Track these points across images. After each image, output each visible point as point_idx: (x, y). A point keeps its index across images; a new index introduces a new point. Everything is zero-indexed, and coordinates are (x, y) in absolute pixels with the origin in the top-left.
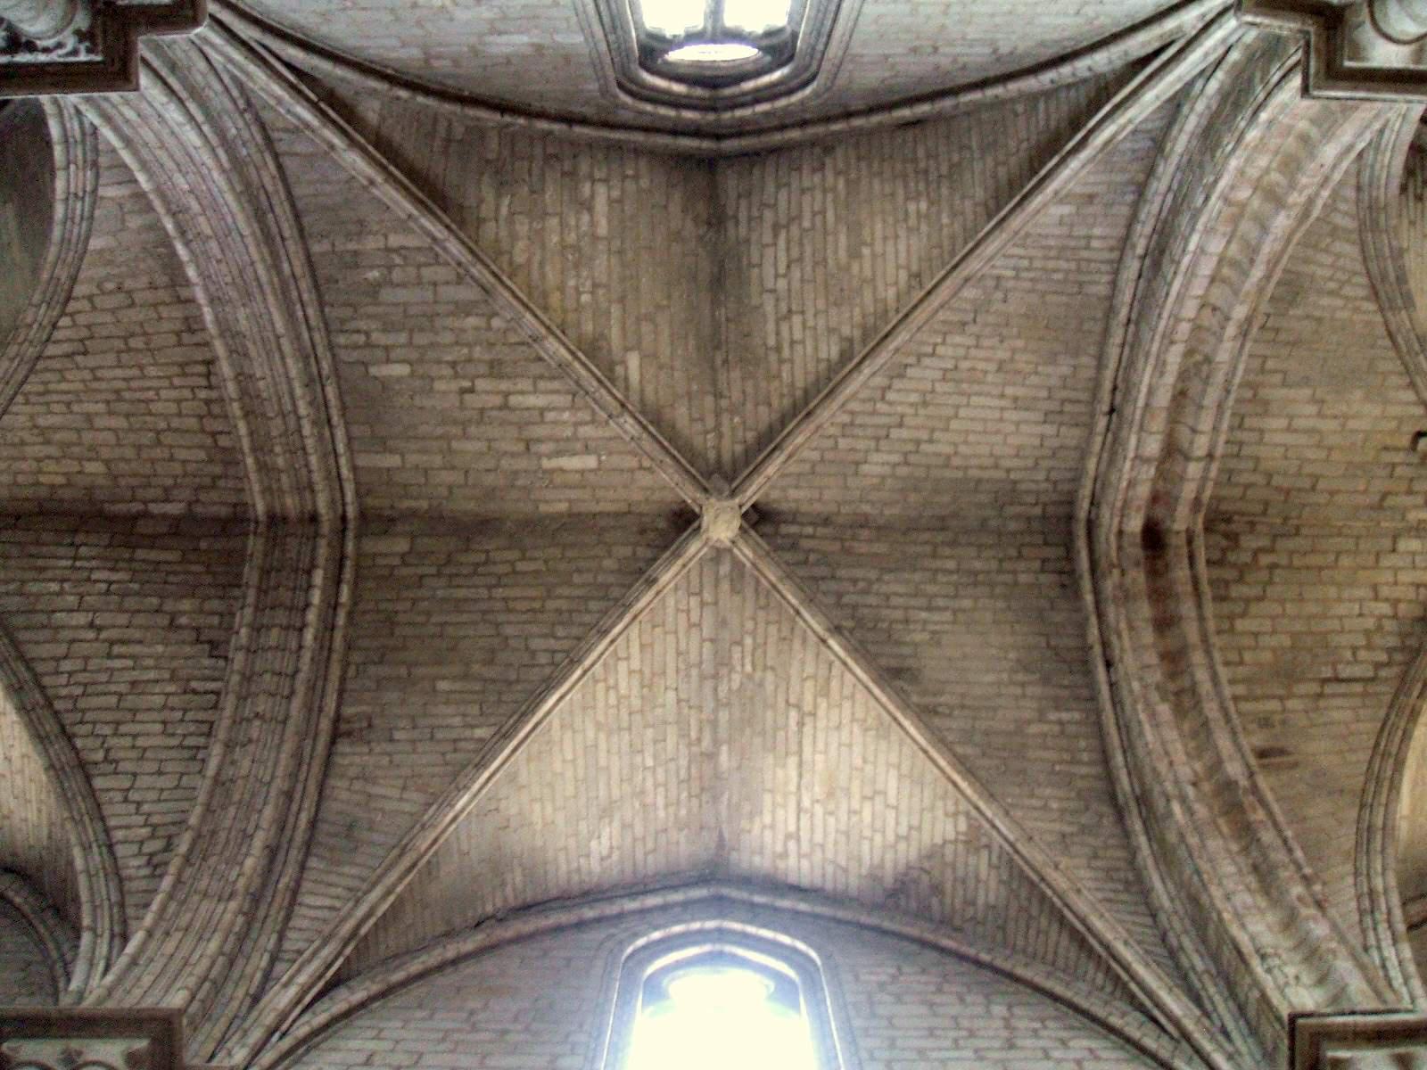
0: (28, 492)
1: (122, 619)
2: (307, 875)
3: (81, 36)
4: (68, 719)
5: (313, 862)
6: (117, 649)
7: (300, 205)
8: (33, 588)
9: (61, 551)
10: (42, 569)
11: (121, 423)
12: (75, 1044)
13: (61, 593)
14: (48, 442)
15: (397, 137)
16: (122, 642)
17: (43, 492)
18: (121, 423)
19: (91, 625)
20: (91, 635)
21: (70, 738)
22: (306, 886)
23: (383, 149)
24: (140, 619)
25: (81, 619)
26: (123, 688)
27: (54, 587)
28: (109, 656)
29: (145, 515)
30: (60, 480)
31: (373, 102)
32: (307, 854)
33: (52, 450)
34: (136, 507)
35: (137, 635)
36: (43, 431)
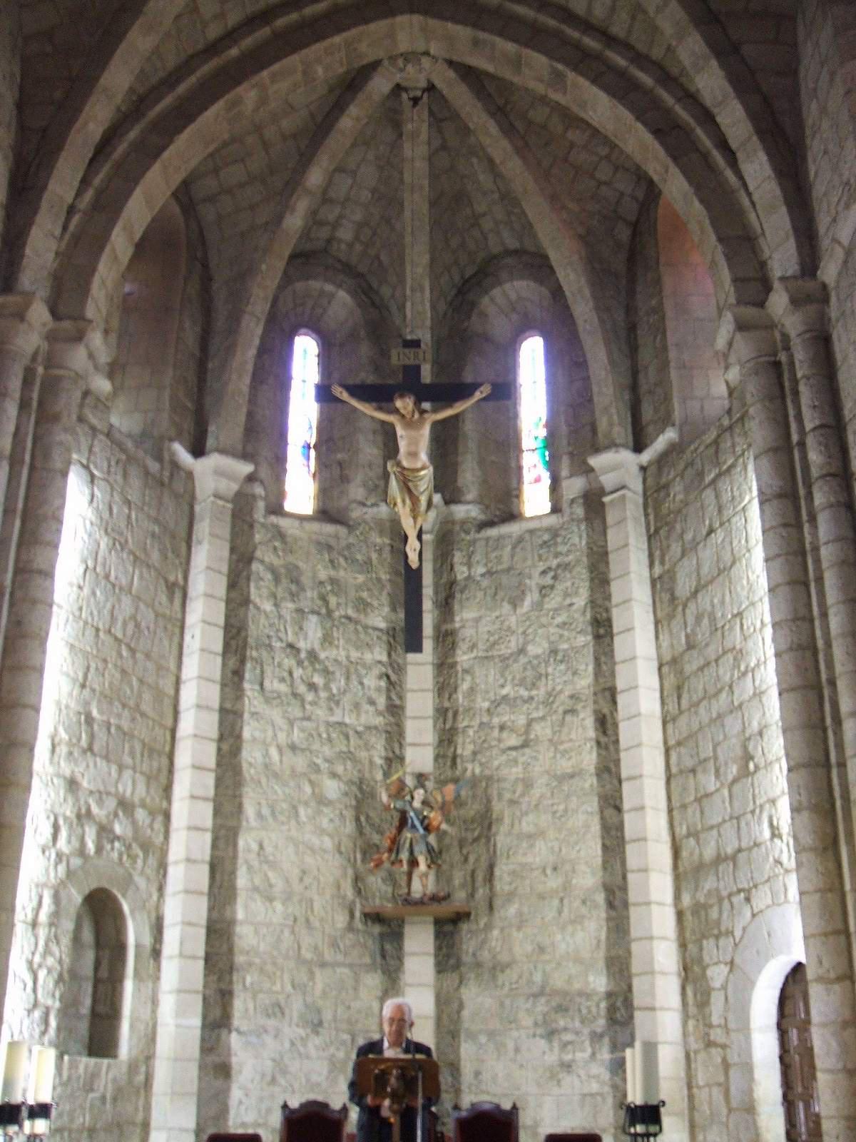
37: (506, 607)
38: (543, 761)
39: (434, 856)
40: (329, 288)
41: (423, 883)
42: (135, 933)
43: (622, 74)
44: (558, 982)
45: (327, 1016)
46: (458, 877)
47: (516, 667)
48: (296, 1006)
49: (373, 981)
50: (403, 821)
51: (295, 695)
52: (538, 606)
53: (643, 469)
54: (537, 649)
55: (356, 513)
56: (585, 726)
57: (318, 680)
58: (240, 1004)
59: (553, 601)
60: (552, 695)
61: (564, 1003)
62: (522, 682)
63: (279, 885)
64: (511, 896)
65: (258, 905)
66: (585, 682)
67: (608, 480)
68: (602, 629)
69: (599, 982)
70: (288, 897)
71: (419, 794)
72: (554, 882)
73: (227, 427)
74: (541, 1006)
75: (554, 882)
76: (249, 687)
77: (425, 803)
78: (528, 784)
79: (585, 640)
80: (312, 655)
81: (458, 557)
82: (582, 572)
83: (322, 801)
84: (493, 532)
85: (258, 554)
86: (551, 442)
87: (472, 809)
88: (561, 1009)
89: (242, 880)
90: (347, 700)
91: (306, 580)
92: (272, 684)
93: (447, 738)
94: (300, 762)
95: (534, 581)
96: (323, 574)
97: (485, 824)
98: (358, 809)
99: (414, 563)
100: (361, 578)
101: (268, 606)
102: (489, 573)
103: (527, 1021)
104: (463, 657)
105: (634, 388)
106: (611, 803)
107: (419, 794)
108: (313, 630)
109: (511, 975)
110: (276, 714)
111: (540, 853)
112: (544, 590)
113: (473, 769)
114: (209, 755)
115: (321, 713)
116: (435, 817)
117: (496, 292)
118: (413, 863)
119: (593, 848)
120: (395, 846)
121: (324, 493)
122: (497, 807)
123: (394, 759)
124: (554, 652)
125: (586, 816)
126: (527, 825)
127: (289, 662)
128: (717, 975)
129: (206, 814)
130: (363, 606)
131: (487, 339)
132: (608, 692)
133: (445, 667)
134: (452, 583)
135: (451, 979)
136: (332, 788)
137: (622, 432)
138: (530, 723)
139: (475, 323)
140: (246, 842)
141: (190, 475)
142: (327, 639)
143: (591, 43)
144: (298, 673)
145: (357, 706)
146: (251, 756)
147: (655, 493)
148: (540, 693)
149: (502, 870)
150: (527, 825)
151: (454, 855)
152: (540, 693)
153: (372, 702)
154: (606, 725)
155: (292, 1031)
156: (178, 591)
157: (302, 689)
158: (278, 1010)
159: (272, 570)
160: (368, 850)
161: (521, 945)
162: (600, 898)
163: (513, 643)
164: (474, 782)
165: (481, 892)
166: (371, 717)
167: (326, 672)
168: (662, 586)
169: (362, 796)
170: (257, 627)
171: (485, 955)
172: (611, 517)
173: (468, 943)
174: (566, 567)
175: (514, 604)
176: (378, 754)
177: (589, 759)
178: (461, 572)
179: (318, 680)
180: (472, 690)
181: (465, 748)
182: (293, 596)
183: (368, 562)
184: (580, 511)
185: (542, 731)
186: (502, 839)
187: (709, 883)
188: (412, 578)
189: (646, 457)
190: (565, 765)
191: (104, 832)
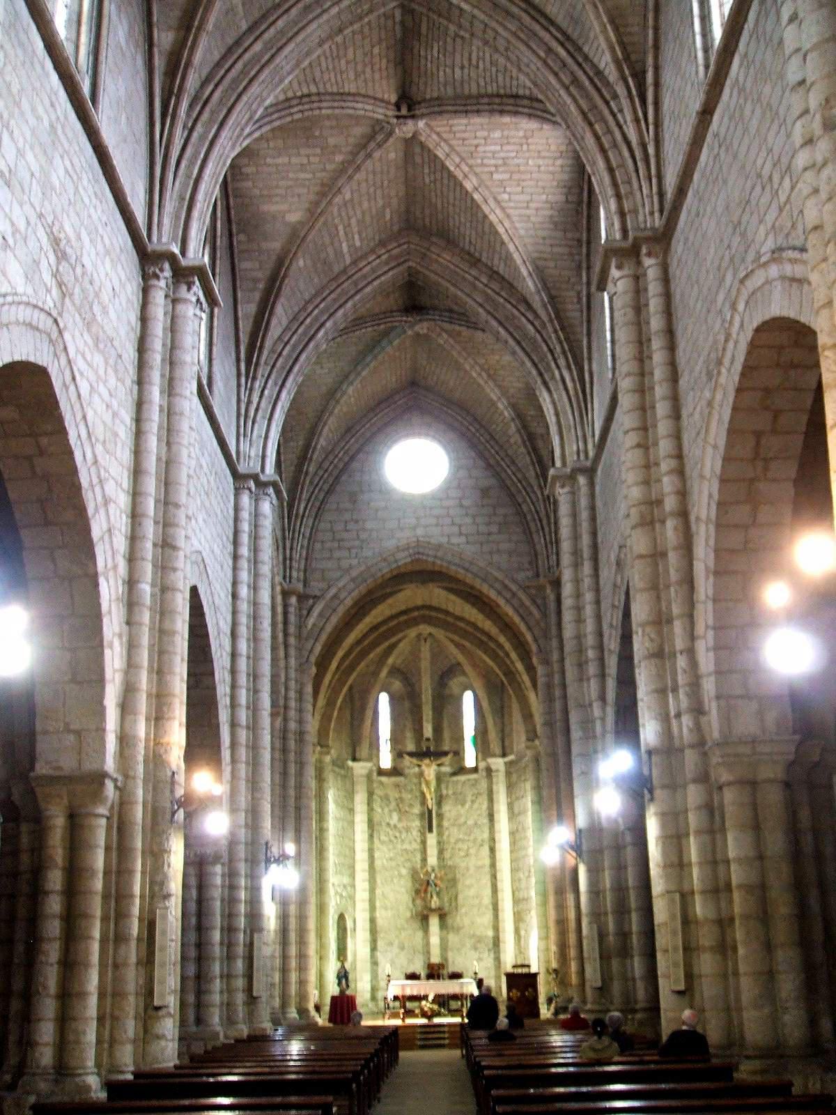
0: (391, 71)
1: (458, 57)
2: (591, 55)
3: (189, 289)
4: (508, 91)
5: (586, 49)
6: (474, 62)
7: (223, 51)
8: (442, 79)
9: (423, 61)
10: (432, 74)
11: (351, 52)
12: (610, 279)
13: (445, 71)
14: (364, 72)
15: (177, 13)
16: (470, 59)
17: (391, 65)
18: (351, 52)
19: (462, 68)
20: (466, 71)
21: (516, 96)
22: (595, 60)
23: (188, 26)
24: (458, 48)
25: (458, 72)
26: (494, 69)
27: (441, 73)
28: (477, 67)
29: (402, 23)
30: (384, 61)
31: (165, 39)
32: (580, 49)
33: (368, 70)
34: (398, 28)
35: (466, 55)
36: (357, 76)
37: (460, 807)
38: (472, 862)
39: (438, 894)
40: (393, 680)
41: (435, 903)
42: (349, 924)
43: (494, 651)
44: (478, 933)
45: (406, 945)
46: (446, 899)
47: (464, 829)
48: (396, 942)
49: (420, 934)
50: (428, 883)
51: (390, 841)
52: (471, 807)
53: (505, 763)
54: (470, 822)
55: (407, 771)
56: (485, 850)
57: (398, 834)
58: (380, 944)
59: (476, 806)
60: (475, 840)
61: (479, 940)
62: (466, 834)
63: (389, 904)
64: (463, 906)
65: (383, 912)
66: (486, 835)
67: (493, 767)
68: (491, 816)
69: (490, 933)
70: (392, 909)
71: (433, 875)
72: (477, 901)
73: (364, 751)
74: (473, 940)
75: (477, 901)
76: (376, 840)
77: (436, 877)
78: (468, 869)
79: (486, 821)
80: (395, 826)
81: (443, 786)
82: (485, 797)
83: (400, 876)
84: (455, 778)
85: (376, 791)
86: (475, 737)
87: (450, 876)
88: (479, 941)
89: (378, 904)
90: (407, 841)
91: (391, 799)
92: (383, 838)
93: (441, 852)
94: (393, 864)
95: (469, 798)
96: (397, 796)
97: (453, 882)
98: (413, 876)
99: (430, 807)
100: (410, 796)
101: (380, 810)
102: (454, 793)
103: (468, 945)
104: (445, 824)
105: (503, 731)
106: (494, 877)
107: (433, 875)
108: (395, 816)
109: (462, 932)
110: (385, 849)
111: (472, 892)
112: (473, 802)
113: (450, 863)
114: (366, 866)
115: (399, 846)
116: (438, 882)
117: (455, 680)
118: (432, 896)
119: (488, 892)
120: (426, 891)
121: (394, 760)
122: (458, 876)
123: (424, 860)
124: (476, 824)
125: (486, 880)
126: (468, 882)
127: (388, 830)
128: (523, 933)
129: (366, 885)
130: (411, 806)
131: (451, 696)
132: (493, 840)
133: (440, 834)
134: (441, 796)
135: (445, 932)
136: (404, 871)
137: (498, 750)
138: (468, 848)
139: (447, 691)
140: (378, 892)
141: (352, 768)
142: (400, 820)
143: (484, 638)
144: (391, 833)
145: (410, 843)
146: (378, 863)
147: (508, 774)
148: (472, 838)
149: (460, 897)
150: (468, 882)
151: (444, 893)
152: (472, 838)
153: (415, 841)
154: (492, 850)
155: (395, 950)
156: (351, 811)
157: (393, 838)
158: (391, 944)
159: (381, 798)
160: (417, 892)
161: (466, 921)
162: (491, 907)
163: (462, 820)
164: (450, 867)
165: (453, 904)
166: (416, 846)
167: (400, 832)
168: (510, 806)
169: (414, 874)
170: (376, 818)
171: (455, 925)
172: (494, 780)
173: (449, 921)
174: (479, 794)
175: (463, 805)
176: (418, 857)
177: (487, 862)
178: (444, 792)
179: (398, 834)
180: (449, 836)
181: (447, 855)
182: (388, 806)
183: (412, 790)
184: (484, 774)
185: (472, 851)
186: (460, 886)
187: (521, 906)
188: (430, 812)
189: (507, 759)
190: (480, 863)
191: (341, 896)
